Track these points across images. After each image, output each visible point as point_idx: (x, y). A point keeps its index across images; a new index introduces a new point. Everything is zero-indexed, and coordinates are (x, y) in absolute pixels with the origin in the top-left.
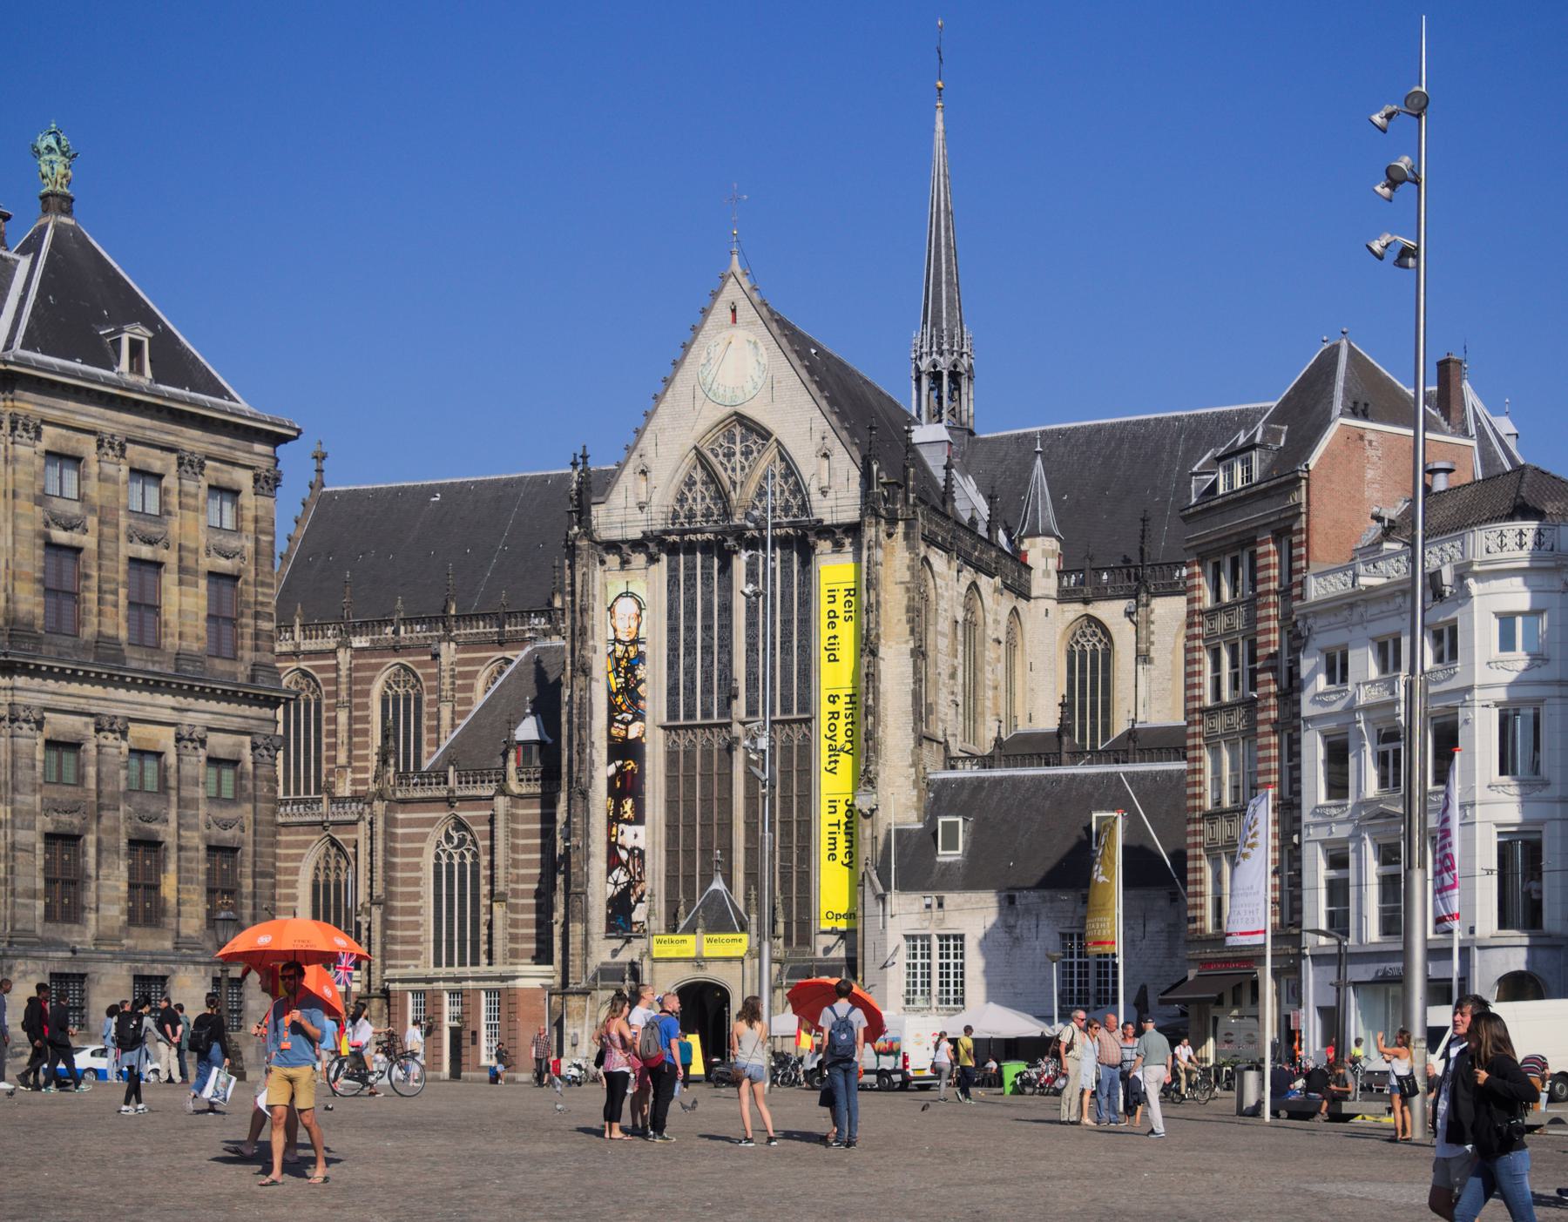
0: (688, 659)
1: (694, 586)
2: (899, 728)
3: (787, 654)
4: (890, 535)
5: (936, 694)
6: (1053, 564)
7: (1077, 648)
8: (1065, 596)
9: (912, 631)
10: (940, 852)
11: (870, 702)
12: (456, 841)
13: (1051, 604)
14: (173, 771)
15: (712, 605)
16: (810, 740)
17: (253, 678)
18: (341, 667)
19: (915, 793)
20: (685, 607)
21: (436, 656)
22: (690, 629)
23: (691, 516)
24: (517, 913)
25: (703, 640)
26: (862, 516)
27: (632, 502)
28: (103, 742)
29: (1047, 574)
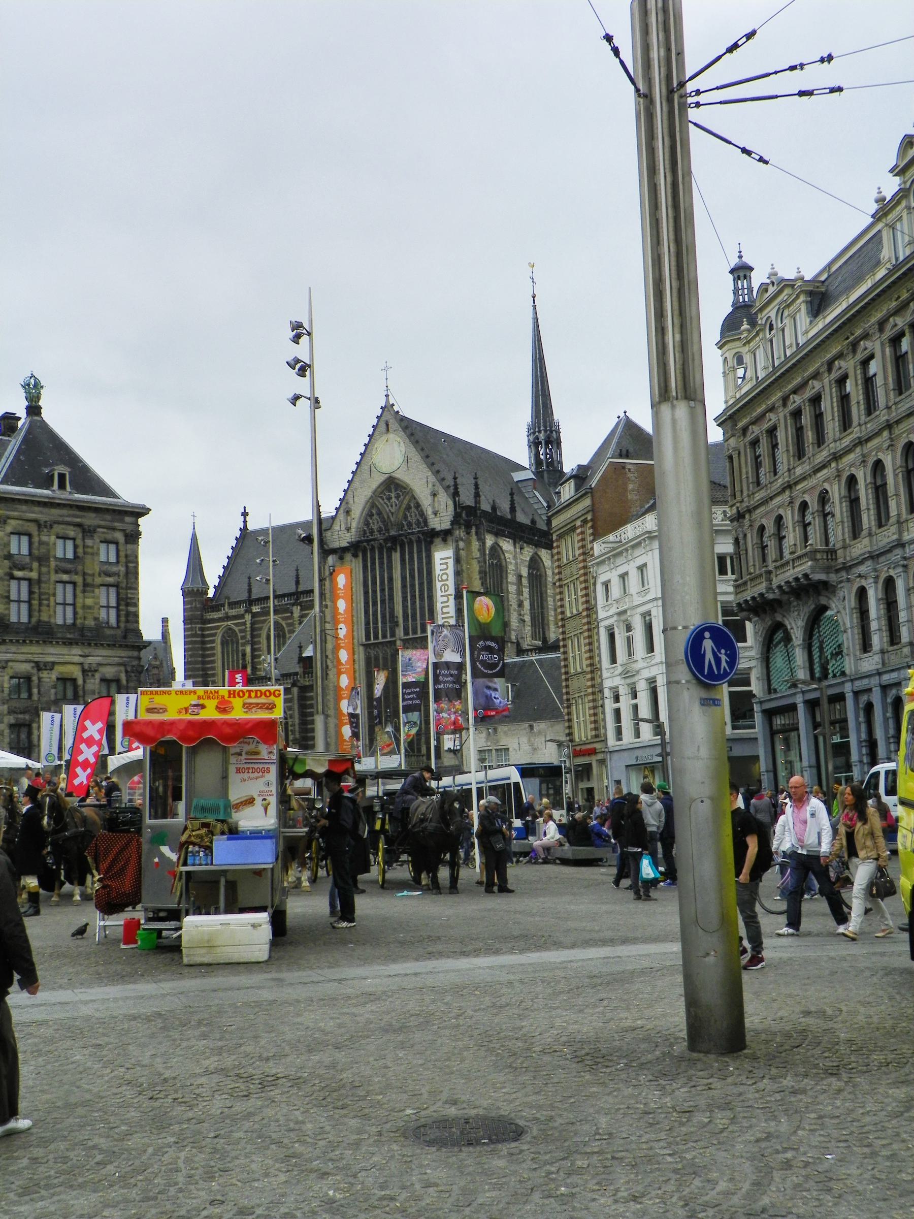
4: (468, 533)
5: (509, 616)
14: (81, 687)
17: (125, 637)
21: (292, 613)
22: (374, 592)
23: (372, 532)
26: (452, 523)
27: (343, 527)
28: (41, 675)
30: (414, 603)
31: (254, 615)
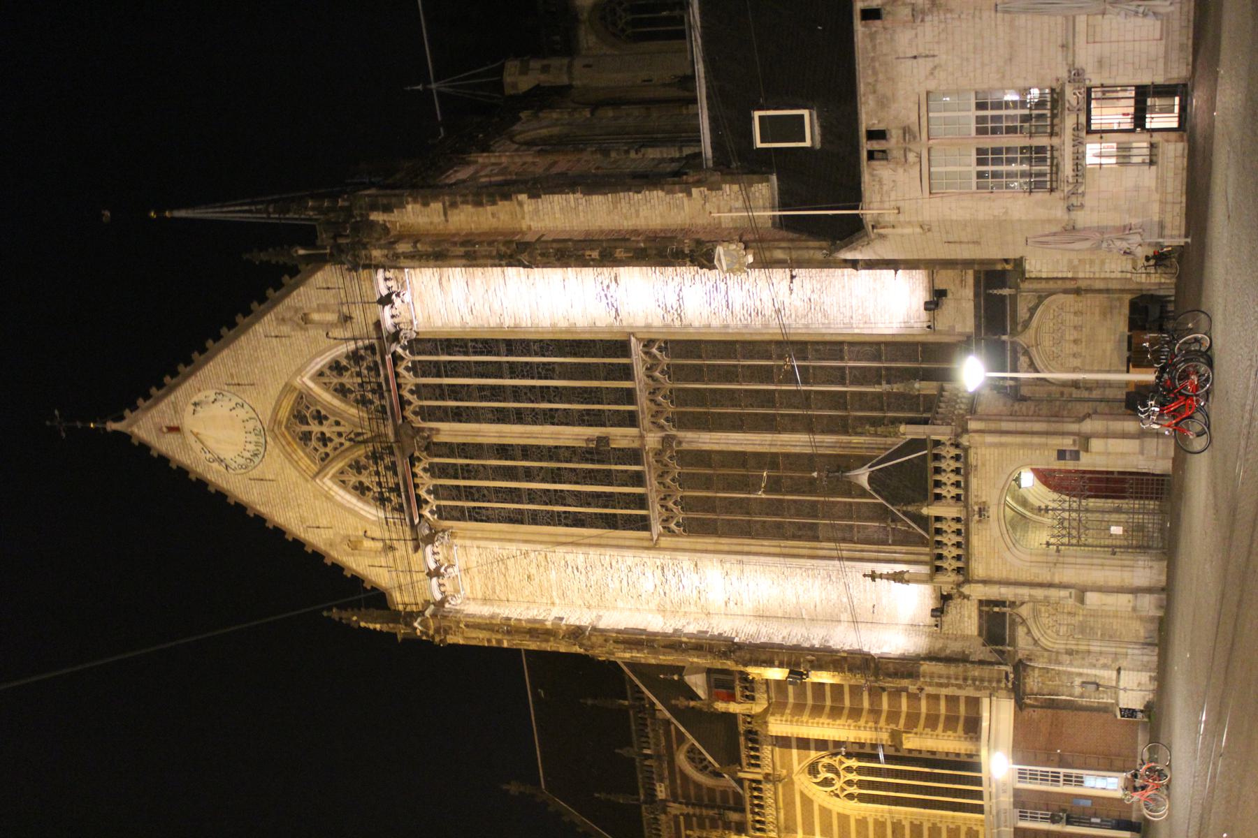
0: (569, 500)
1: (479, 489)
2: (637, 212)
3: (553, 370)
6: (535, 64)
7: (629, 31)
8: (569, 49)
9: (507, 197)
10: (808, 143)
11: (595, 254)
12: (830, 775)
13: (578, 63)
15: (500, 467)
16: (666, 342)
18: (685, 812)
19: (726, 187)
20: (505, 501)
24: (918, 715)
25: (543, 481)
29: (545, 69)
30: (558, 394)
31: (674, 797)
